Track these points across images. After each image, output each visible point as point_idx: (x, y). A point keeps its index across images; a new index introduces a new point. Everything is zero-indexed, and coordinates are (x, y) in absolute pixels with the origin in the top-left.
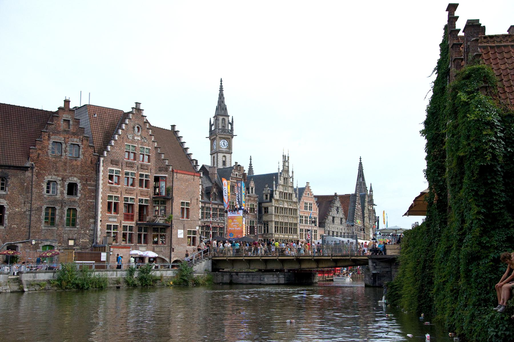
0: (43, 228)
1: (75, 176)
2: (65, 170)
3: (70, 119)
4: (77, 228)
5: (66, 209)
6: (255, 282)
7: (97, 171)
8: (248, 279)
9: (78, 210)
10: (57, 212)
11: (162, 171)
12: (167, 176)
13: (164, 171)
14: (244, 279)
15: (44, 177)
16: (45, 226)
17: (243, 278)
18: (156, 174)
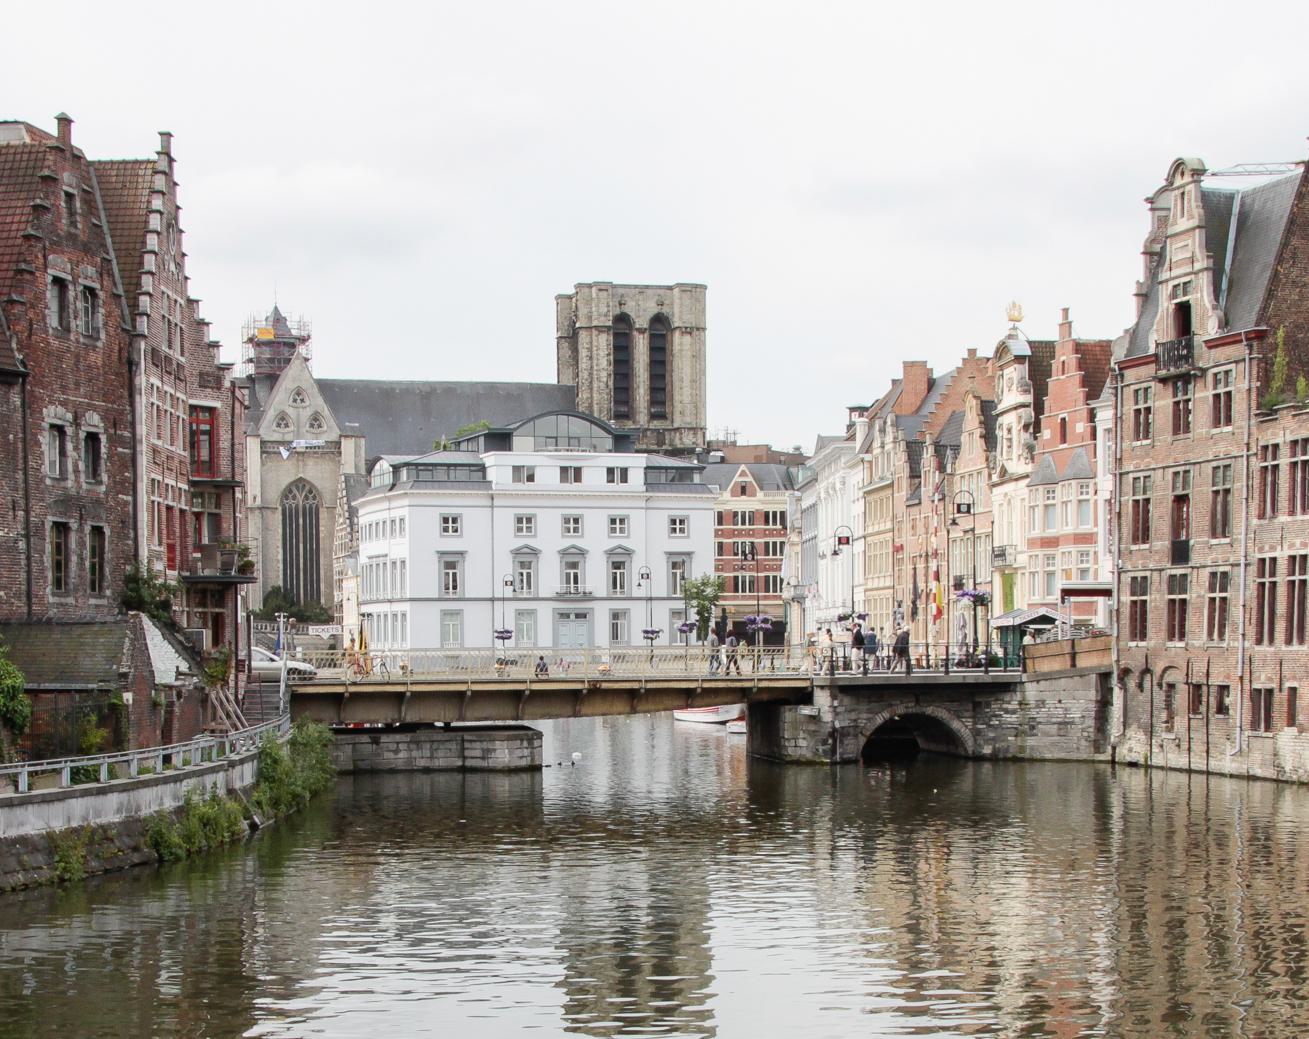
0: (51, 599)
1: (95, 409)
2: (77, 384)
3: (75, 192)
4: (108, 598)
5: (87, 529)
6: (441, 763)
7: (131, 390)
8: (415, 754)
9: (107, 531)
10: (73, 538)
11: (206, 387)
12: (217, 404)
13: (212, 388)
14: (401, 755)
15: (41, 412)
16: (54, 595)
17: (397, 751)
18: (192, 396)
